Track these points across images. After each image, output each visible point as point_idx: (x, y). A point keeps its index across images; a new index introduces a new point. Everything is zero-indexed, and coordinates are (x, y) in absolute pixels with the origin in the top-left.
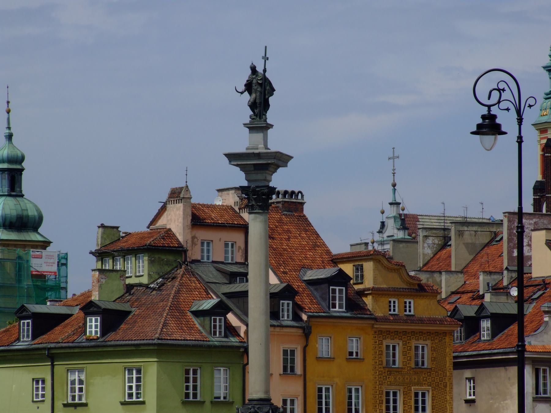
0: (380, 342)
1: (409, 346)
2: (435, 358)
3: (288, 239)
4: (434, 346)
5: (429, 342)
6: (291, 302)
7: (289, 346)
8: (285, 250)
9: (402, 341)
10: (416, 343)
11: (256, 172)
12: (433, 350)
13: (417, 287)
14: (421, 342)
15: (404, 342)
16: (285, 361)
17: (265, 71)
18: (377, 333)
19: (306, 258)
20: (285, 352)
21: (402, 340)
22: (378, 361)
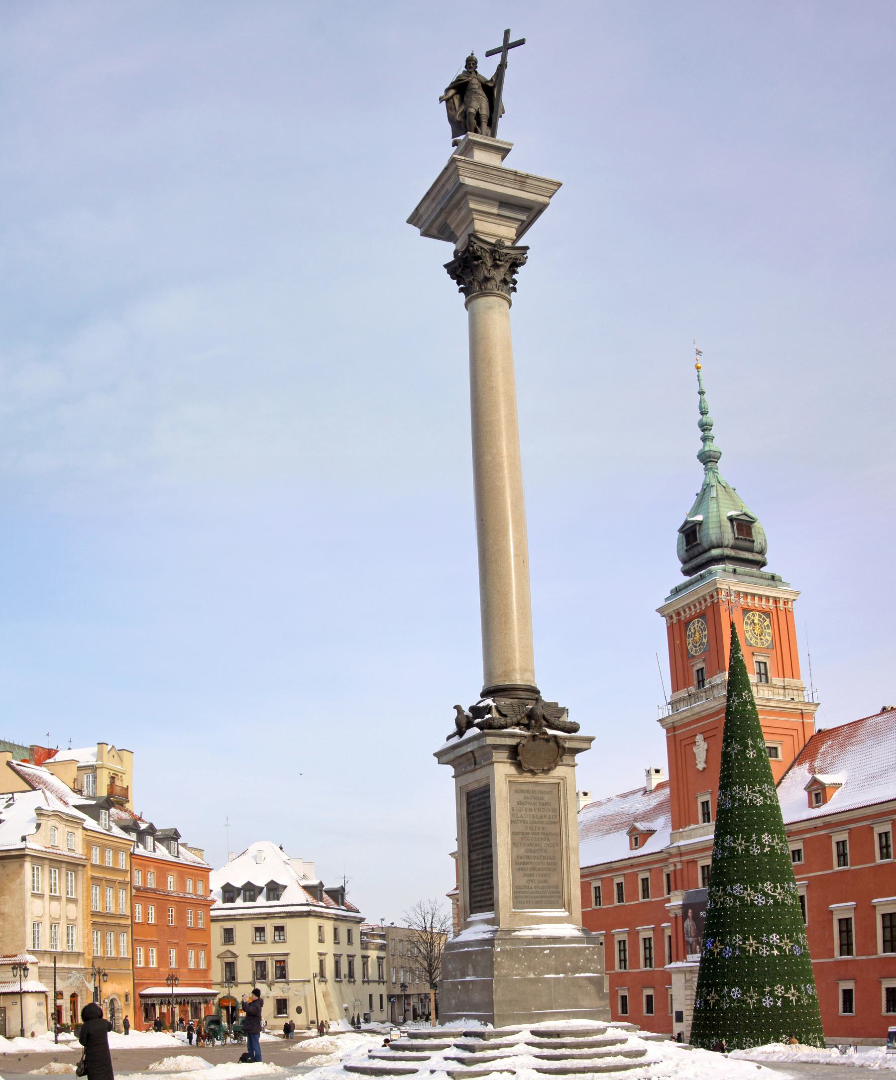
11: (498, 221)
17: (502, 67)
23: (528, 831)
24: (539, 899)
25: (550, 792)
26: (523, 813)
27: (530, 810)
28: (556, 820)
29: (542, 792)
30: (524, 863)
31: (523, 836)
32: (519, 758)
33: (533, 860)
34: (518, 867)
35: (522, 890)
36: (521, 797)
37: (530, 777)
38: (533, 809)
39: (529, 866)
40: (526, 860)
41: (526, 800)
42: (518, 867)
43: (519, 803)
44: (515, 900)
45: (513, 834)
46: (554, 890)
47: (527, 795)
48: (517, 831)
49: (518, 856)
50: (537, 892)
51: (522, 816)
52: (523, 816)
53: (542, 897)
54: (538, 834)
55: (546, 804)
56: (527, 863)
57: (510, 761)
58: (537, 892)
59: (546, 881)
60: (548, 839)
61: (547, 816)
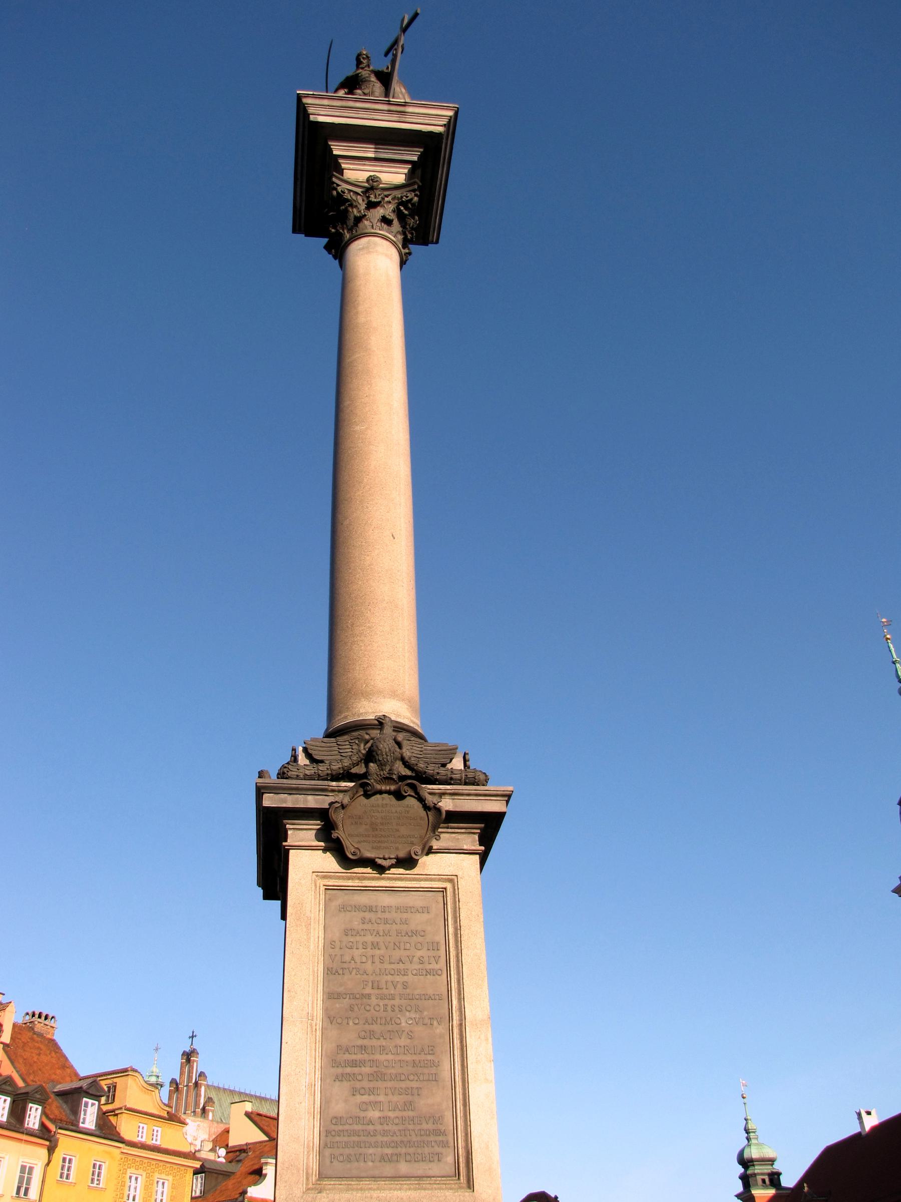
0: (124, 1170)
1: (152, 1180)
2: (174, 1197)
3: (39, 1054)
4: (175, 1183)
5: (170, 1178)
6: (40, 1108)
7: (29, 1161)
8: (35, 1062)
9: (145, 1173)
10: (159, 1177)
12: (174, 1187)
13: (166, 1115)
14: (163, 1176)
15: (148, 1175)
16: (21, 1179)
18: (123, 1160)
19: (55, 1074)
20: (23, 1168)
21: (145, 1171)
22: (119, 1193)
23: (368, 990)
24: (389, 1151)
25: (426, 910)
26: (357, 953)
27: (375, 946)
28: (437, 967)
29: (406, 909)
30: (354, 1064)
31: (353, 1001)
32: (334, 835)
33: (377, 1056)
34: (340, 1070)
35: (347, 1127)
36: (355, 920)
37: (373, 879)
38: (382, 945)
39: (366, 1070)
40: (359, 1057)
41: (366, 926)
42: (340, 1070)
43: (346, 932)
44: (327, 1152)
45: (331, 996)
46: (430, 1126)
47: (368, 915)
48: (341, 989)
49: (339, 1047)
50: (385, 1133)
51: (353, 959)
52: (357, 959)
53: (396, 1145)
54: (392, 998)
55: (415, 933)
56: (362, 1063)
57: (322, 844)
58: (385, 1133)
59: (408, 1106)
60: (418, 1010)
61: (416, 959)
